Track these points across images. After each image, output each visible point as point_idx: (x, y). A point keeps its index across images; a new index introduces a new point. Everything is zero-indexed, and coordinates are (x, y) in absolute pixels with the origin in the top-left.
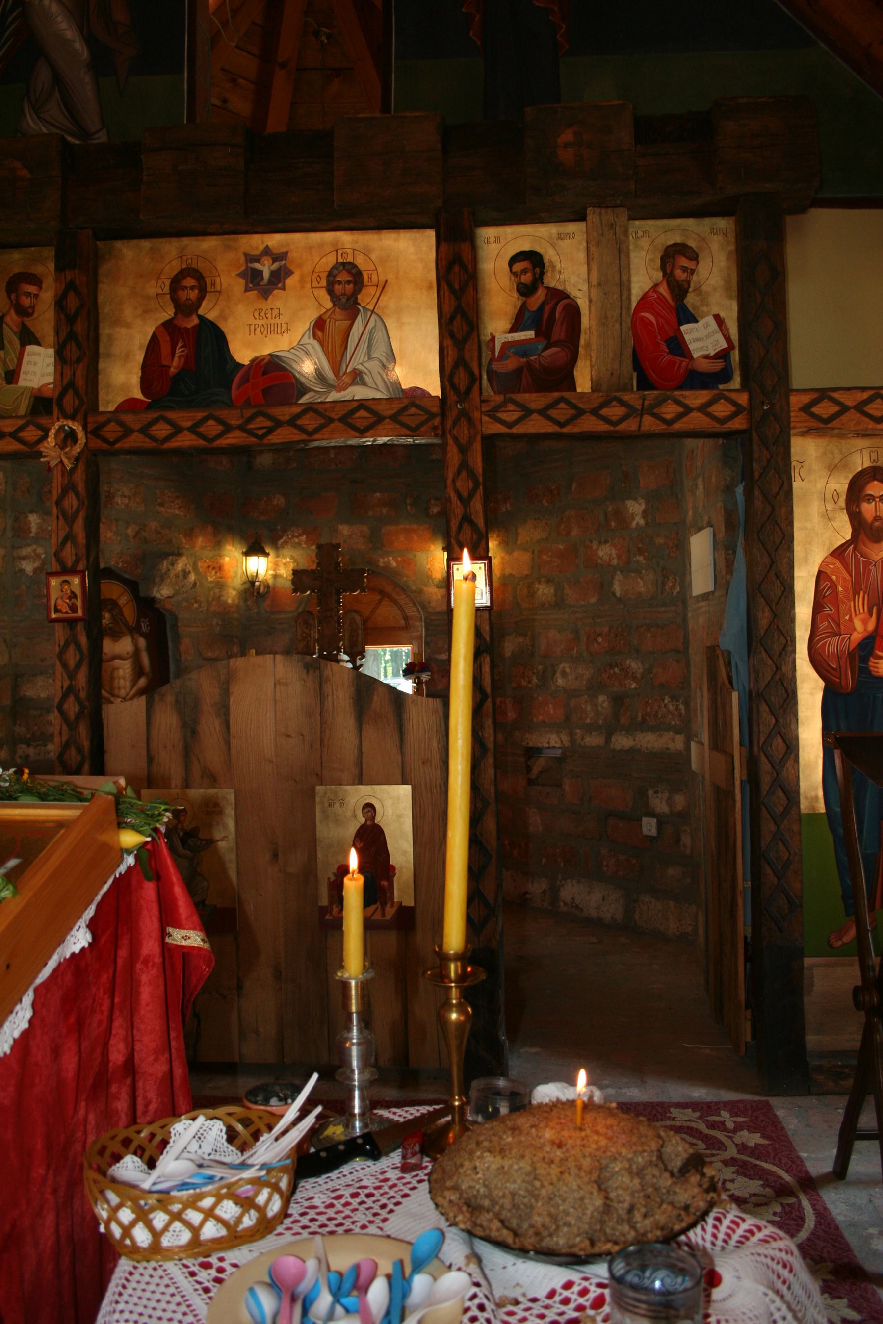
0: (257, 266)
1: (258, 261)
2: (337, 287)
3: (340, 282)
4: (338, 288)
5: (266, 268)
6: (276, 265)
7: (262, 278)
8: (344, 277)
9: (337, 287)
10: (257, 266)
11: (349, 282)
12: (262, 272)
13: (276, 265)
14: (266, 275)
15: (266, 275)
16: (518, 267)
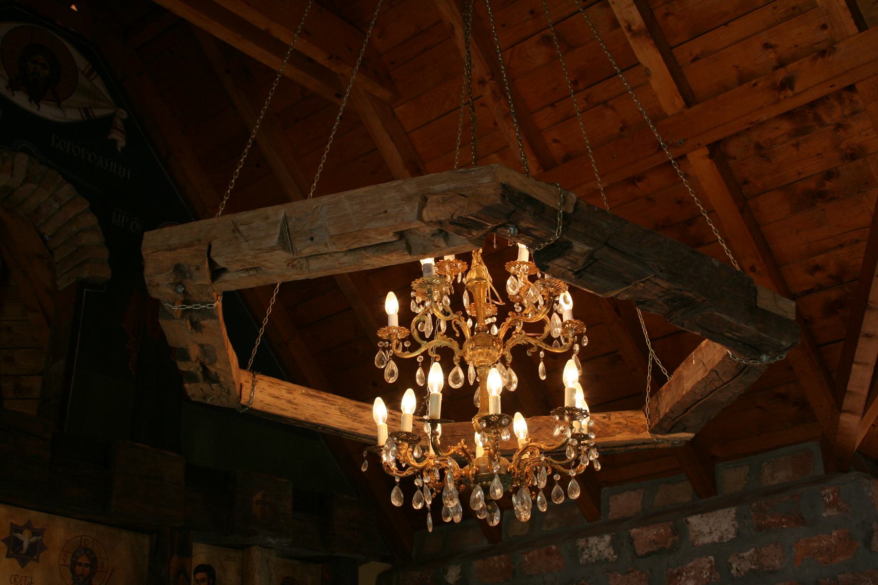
0: (19, 535)
1: (21, 532)
2: (78, 567)
3: (80, 564)
4: (79, 569)
5: (26, 539)
6: (34, 539)
7: (22, 548)
8: (84, 560)
9: (78, 567)
10: (19, 535)
11: (87, 565)
12: (22, 542)
13: (34, 539)
14: (26, 545)
15: (26, 545)
16: (200, 576)
